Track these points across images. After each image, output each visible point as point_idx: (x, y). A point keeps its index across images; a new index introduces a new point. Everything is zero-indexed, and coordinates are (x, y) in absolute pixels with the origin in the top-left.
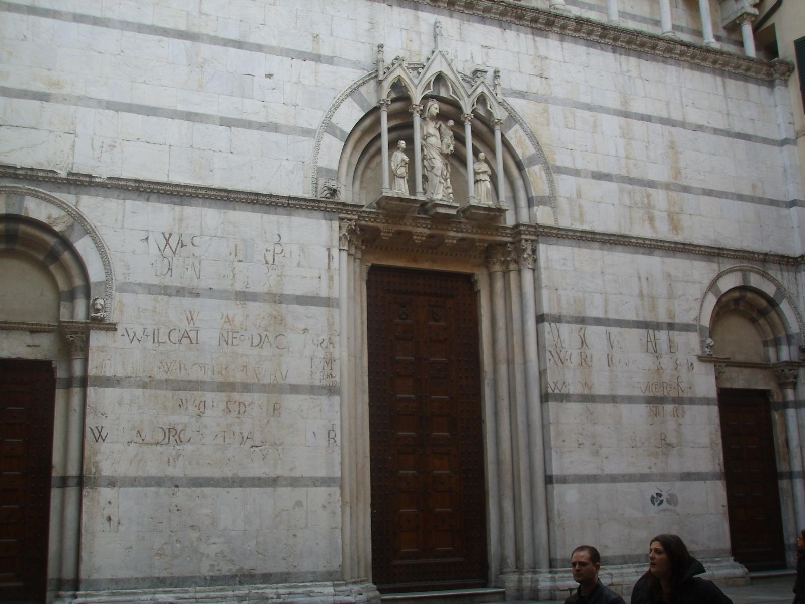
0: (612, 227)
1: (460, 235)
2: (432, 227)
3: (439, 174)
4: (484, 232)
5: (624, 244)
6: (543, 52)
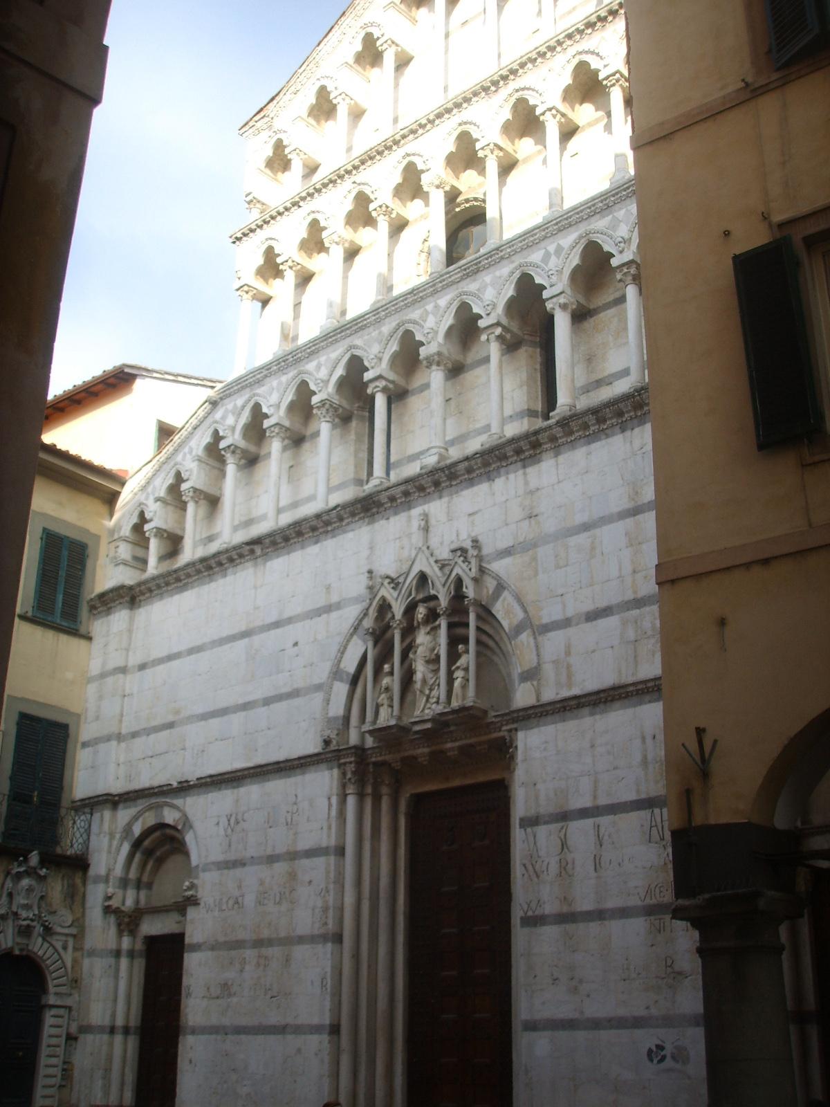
1: (457, 744)
5: (620, 698)
6: (533, 484)
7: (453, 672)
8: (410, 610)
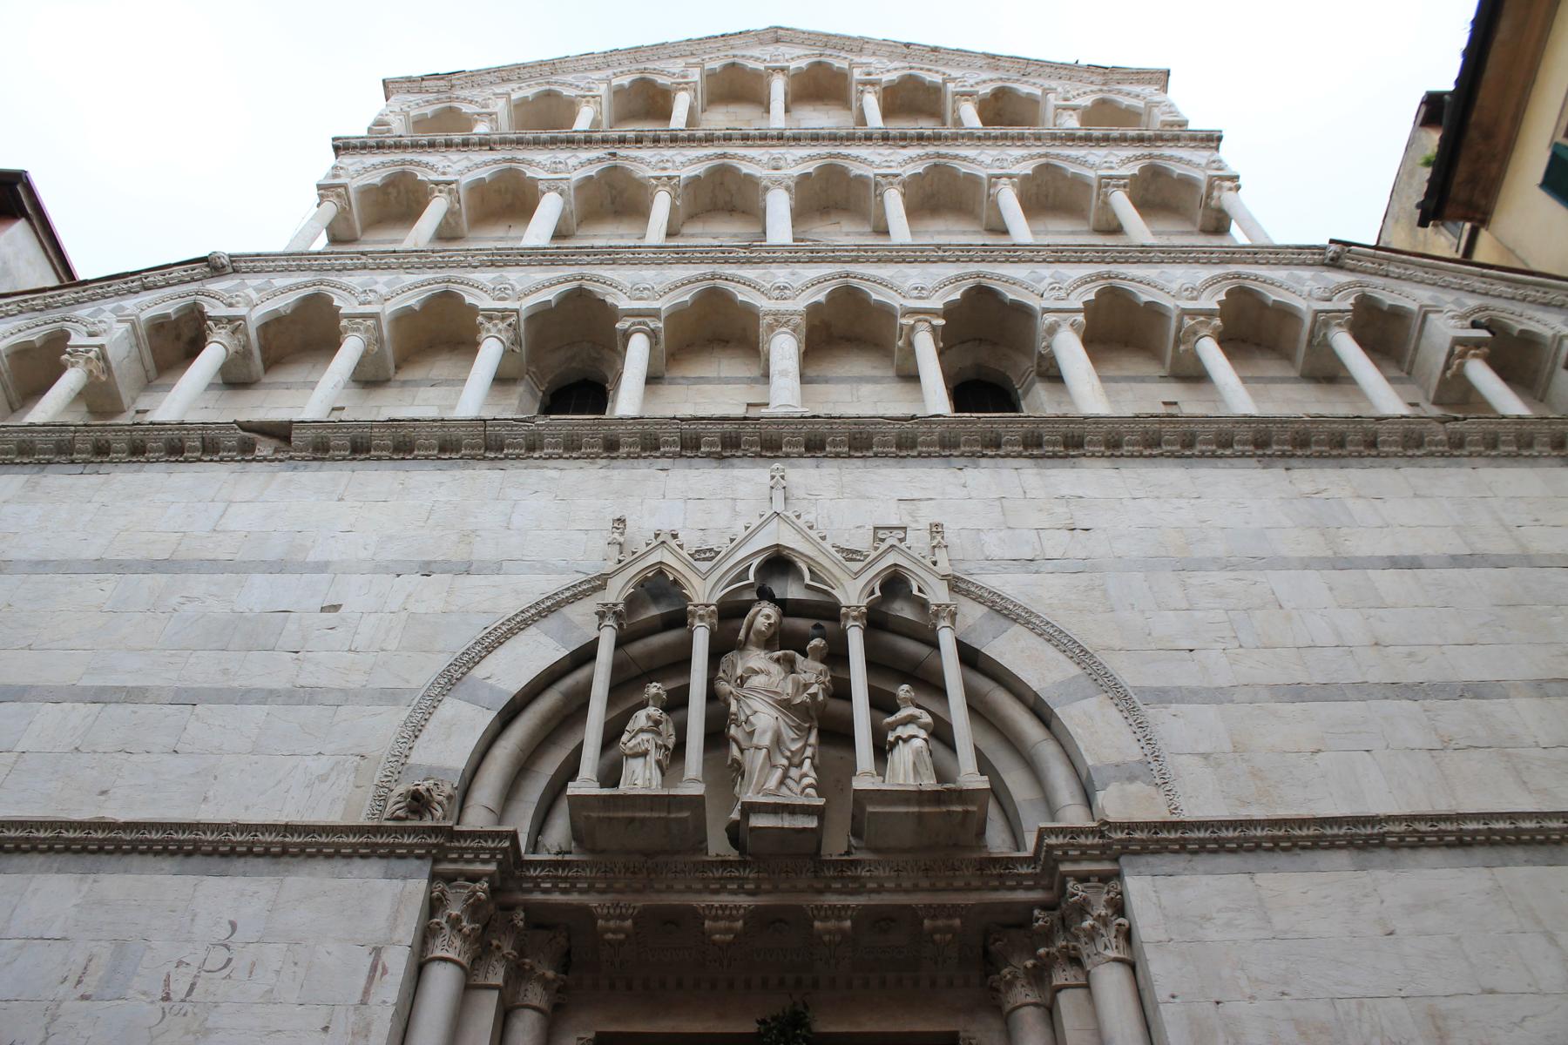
0: (1380, 800)
2: (758, 887)
3: (766, 740)
7: (893, 727)
8: (731, 612)
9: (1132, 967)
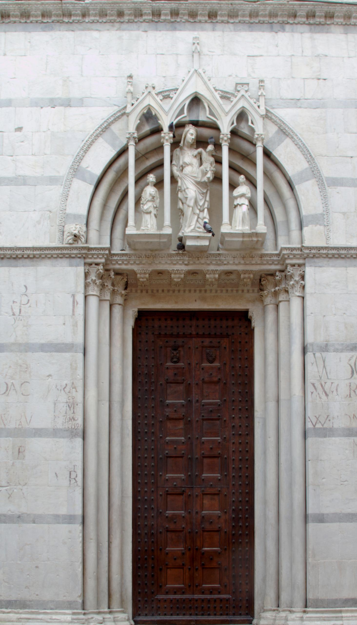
4: (248, 263)
9: (303, 298)
